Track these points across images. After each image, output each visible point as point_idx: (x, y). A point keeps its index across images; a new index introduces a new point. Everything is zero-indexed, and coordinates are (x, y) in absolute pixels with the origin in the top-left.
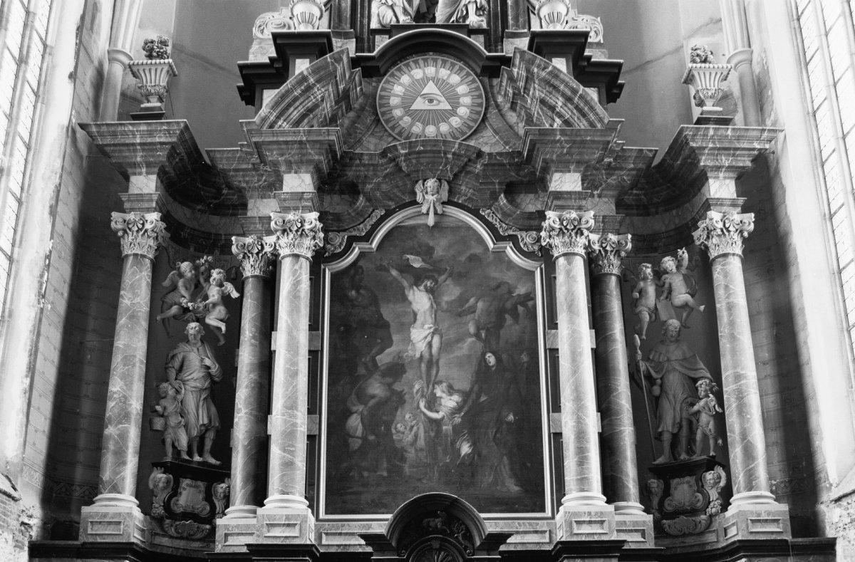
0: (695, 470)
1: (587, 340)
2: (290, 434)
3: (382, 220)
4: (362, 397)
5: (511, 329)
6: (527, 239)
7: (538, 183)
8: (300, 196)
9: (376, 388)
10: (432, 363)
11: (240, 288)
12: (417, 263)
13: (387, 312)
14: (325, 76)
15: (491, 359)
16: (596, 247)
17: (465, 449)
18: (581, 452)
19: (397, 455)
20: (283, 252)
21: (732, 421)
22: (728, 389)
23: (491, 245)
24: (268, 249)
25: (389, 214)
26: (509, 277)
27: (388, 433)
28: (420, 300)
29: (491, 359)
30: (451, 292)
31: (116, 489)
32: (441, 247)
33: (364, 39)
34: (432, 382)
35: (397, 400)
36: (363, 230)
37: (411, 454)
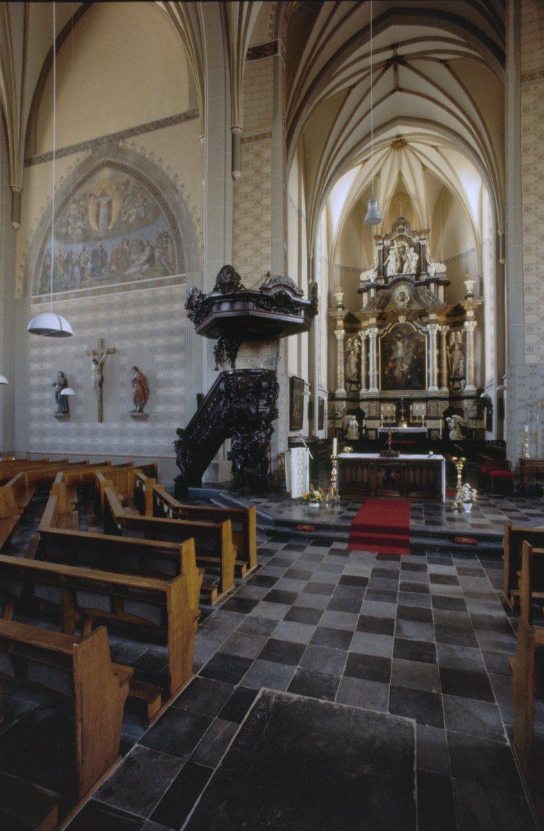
0: (459, 380)
1: (436, 352)
2: (373, 376)
3: (391, 326)
4: (388, 367)
5: (420, 350)
6: (424, 329)
7: (427, 315)
8: (373, 324)
9: (390, 364)
10: (402, 359)
11: (361, 342)
12: (399, 335)
13: (393, 348)
14: (377, 295)
15: (415, 357)
16: (440, 329)
17: (409, 377)
18: (433, 378)
19: (394, 378)
20: (371, 337)
21: (467, 370)
22: (468, 363)
23: (416, 330)
24: (367, 334)
25: (393, 324)
26: (420, 338)
27: (393, 375)
28: (400, 344)
29: (415, 357)
30: (407, 342)
31: (341, 387)
32: (405, 332)
33: (386, 279)
34: (402, 363)
35: (395, 367)
36: (387, 328)
37: (398, 379)
